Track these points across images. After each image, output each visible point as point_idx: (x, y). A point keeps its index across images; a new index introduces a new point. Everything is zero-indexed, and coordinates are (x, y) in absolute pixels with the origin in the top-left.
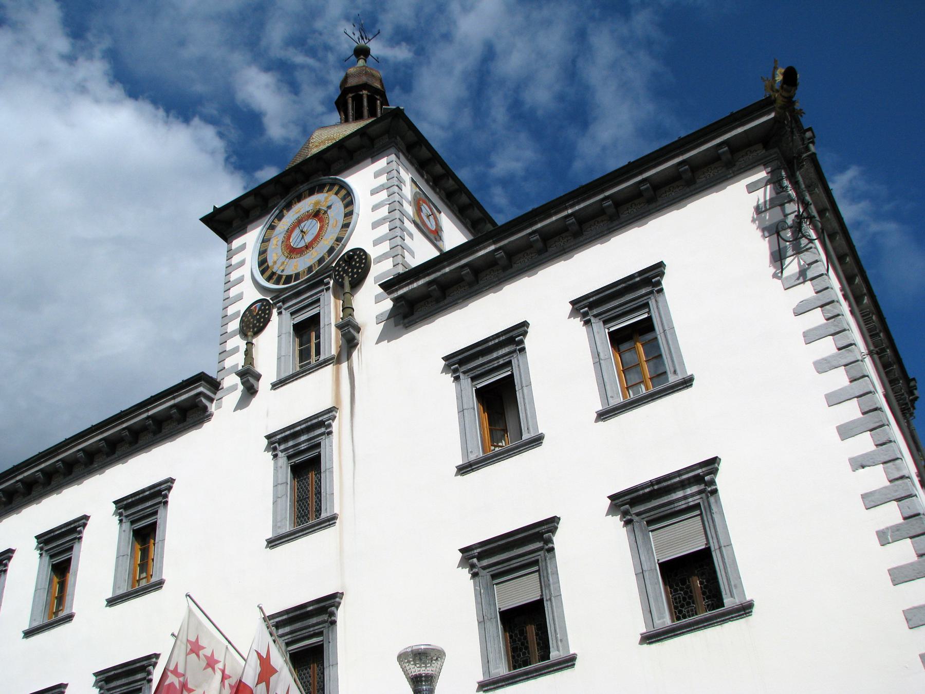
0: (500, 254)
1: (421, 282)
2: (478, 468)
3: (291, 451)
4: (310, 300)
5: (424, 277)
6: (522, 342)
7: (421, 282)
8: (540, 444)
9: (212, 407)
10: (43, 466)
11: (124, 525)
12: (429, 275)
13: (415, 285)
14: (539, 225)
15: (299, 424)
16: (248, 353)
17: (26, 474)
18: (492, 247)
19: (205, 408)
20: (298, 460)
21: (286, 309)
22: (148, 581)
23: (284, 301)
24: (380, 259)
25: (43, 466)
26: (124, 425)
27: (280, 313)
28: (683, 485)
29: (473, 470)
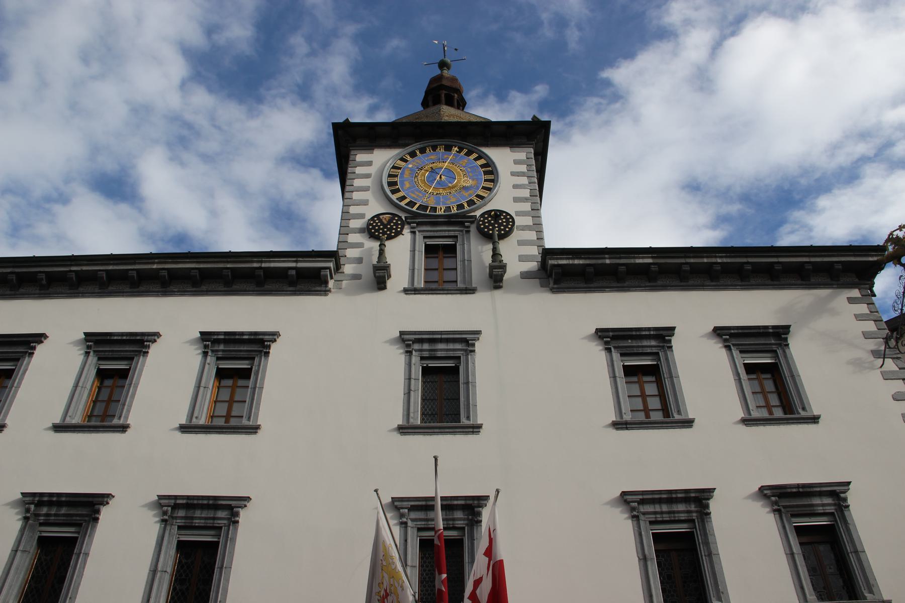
0: (653, 268)
1: (581, 262)
2: (632, 429)
3: (426, 354)
4: (452, 234)
5: (585, 258)
6: (670, 341)
7: (581, 262)
8: (691, 426)
9: (331, 284)
10: (111, 268)
11: (209, 358)
12: (589, 258)
13: (576, 262)
14: (692, 260)
15: (441, 333)
16: (382, 252)
17: (84, 268)
18: (650, 261)
19: (326, 283)
20: (433, 364)
21: (419, 231)
22: (227, 421)
23: (419, 224)
24: (524, 228)
25: (111, 268)
26: (229, 266)
27: (413, 233)
28: (821, 494)
29: (627, 429)
